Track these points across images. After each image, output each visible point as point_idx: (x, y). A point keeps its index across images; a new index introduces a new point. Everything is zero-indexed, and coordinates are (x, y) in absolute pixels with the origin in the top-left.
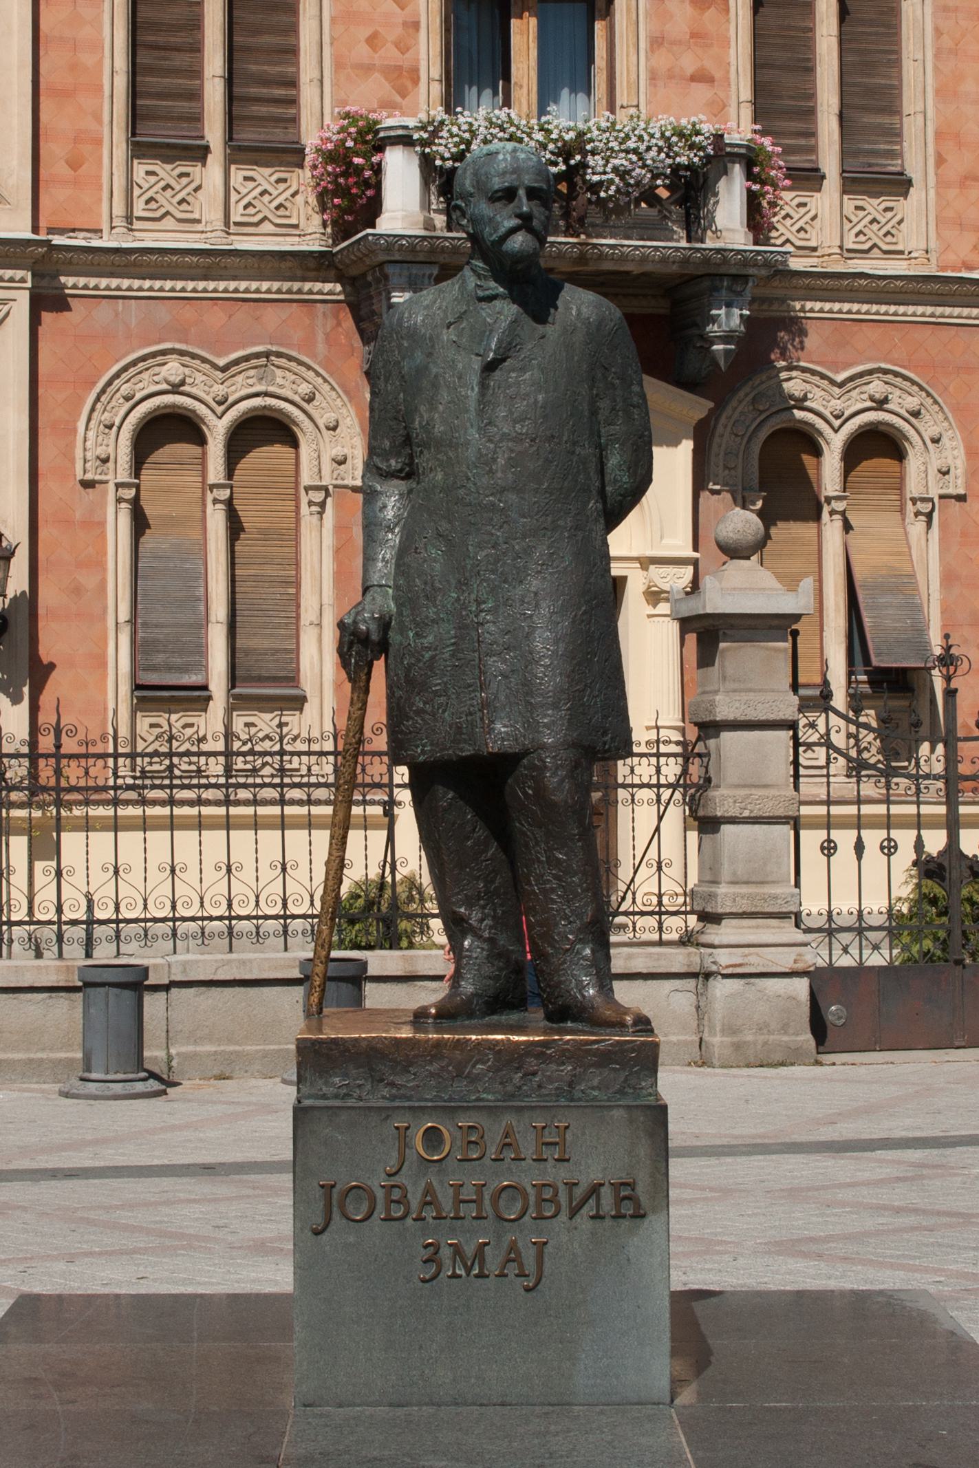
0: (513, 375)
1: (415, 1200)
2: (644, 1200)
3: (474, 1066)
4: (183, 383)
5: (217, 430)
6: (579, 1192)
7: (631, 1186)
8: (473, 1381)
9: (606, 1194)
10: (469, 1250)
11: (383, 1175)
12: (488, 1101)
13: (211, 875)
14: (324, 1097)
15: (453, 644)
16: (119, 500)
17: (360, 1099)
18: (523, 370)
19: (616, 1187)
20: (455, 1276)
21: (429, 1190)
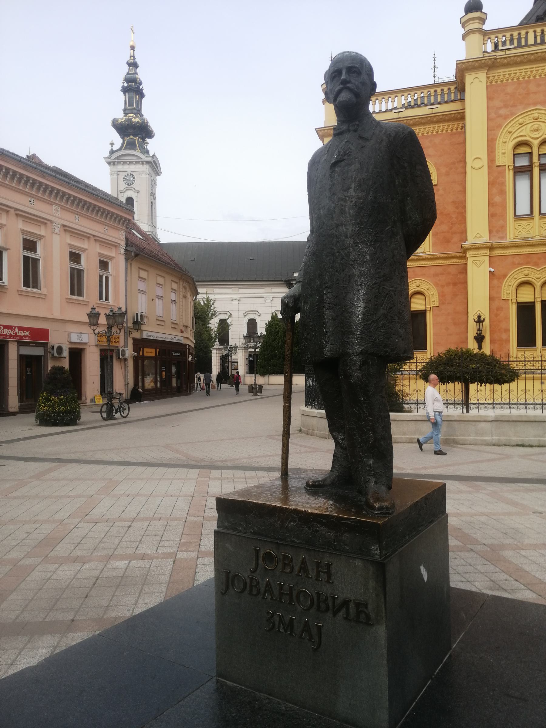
0: (346, 168)
1: (262, 588)
2: (372, 615)
3: (289, 523)
4: (528, 275)
5: (538, 284)
6: (338, 602)
7: (366, 606)
8: (289, 690)
9: (352, 605)
10: (287, 620)
11: (249, 572)
12: (296, 542)
13: (520, 392)
14: (226, 528)
15: (317, 305)
16: (512, 303)
17: (240, 531)
18: (350, 165)
19: (358, 605)
20: (279, 630)
21: (268, 585)
